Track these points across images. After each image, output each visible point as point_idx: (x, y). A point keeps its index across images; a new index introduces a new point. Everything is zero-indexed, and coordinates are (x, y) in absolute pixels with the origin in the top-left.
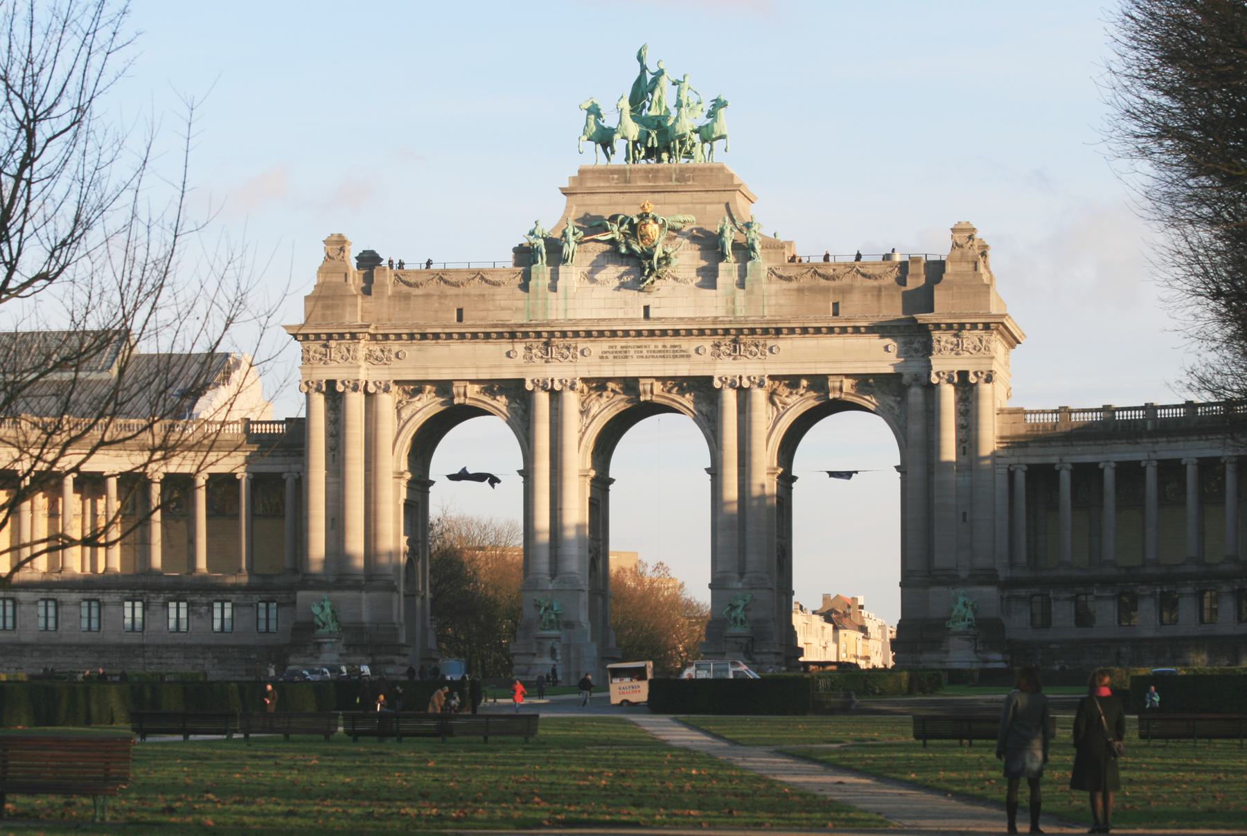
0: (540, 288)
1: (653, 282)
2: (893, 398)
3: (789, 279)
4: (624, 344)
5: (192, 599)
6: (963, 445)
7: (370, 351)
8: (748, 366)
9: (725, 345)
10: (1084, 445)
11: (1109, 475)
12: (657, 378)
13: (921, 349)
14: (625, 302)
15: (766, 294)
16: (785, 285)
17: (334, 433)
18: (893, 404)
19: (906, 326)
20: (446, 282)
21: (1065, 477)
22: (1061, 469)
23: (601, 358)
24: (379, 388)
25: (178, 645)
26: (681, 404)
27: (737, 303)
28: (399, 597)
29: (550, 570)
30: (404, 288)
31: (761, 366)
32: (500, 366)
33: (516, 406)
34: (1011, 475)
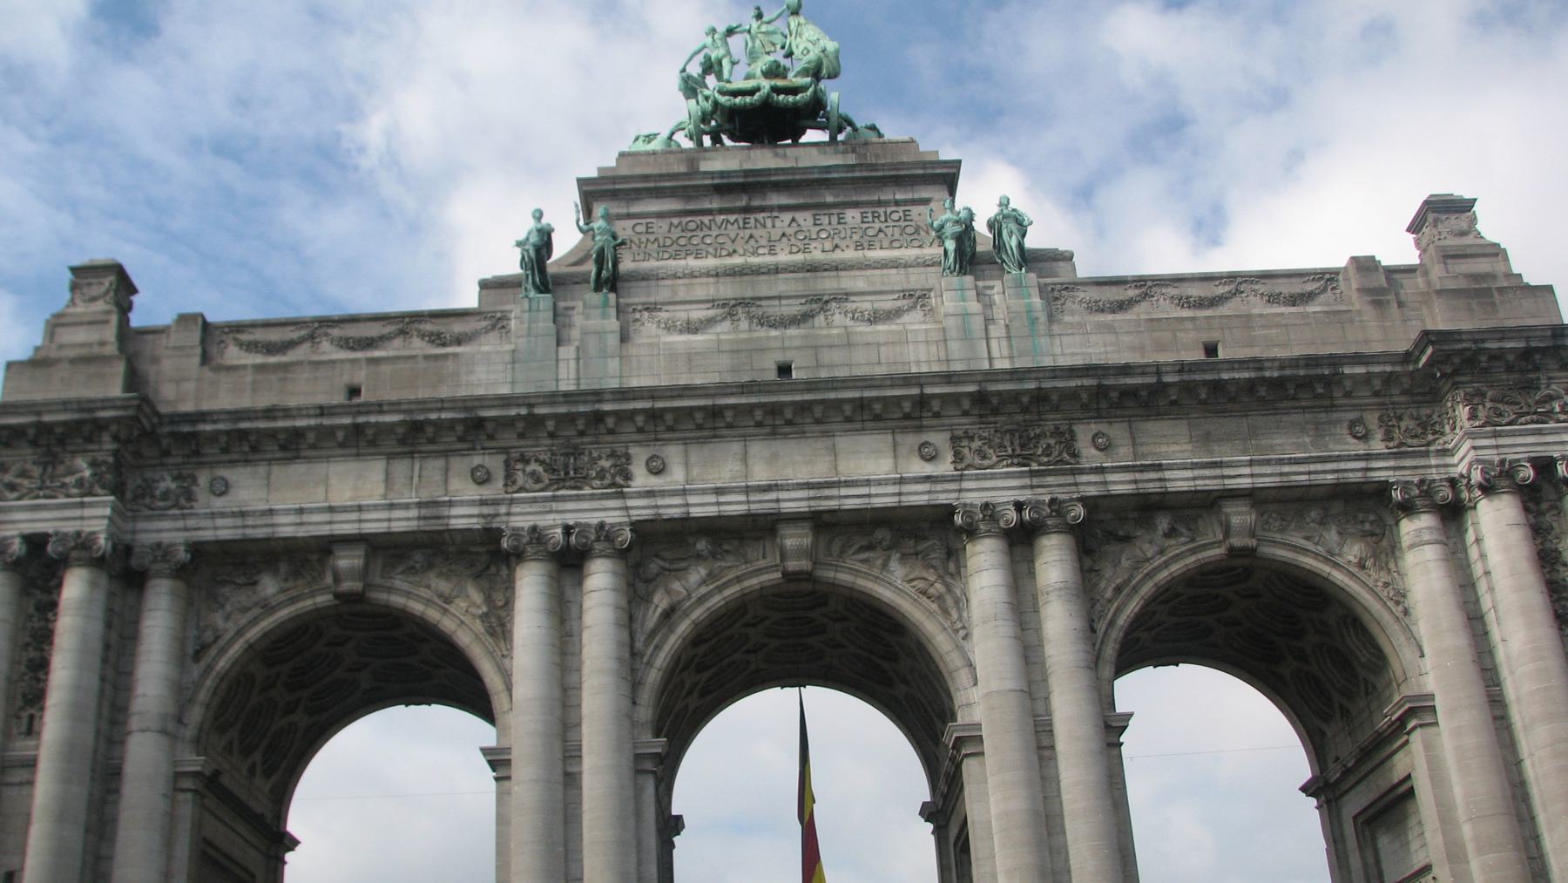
7: (145, 480)
19: (1388, 379)
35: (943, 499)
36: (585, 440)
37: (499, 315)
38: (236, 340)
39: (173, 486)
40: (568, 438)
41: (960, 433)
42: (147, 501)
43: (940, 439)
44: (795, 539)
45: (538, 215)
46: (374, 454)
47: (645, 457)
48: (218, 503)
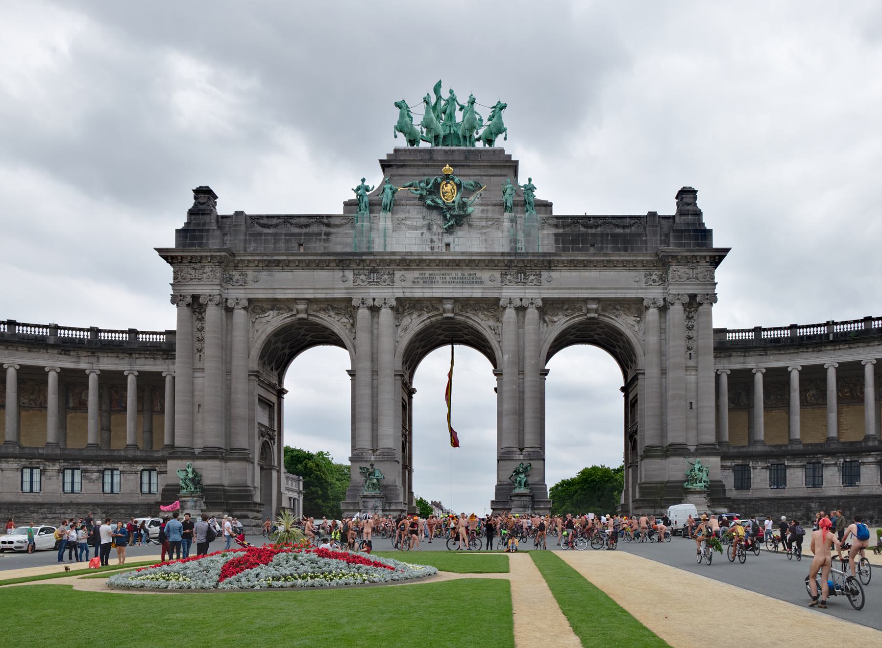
0: (364, 229)
1: (452, 225)
2: (634, 318)
3: (557, 226)
4: (431, 272)
5: (84, 467)
6: (690, 352)
8: (527, 291)
9: (510, 274)
10: (776, 354)
11: (795, 377)
12: (456, 300)
13: (657, 280)
14: (432, 241)
15: (540, 236)
16: (554, 231)
17: (200, 338)
18: (635, 323)
20: (291, 224)
21: (759, 378)
22: (757, 371)
23: (414, 282)
24: (237, 304)
25: (71, 504)
26: (474, 321)
27: (519, 245)
28: (254, 468)
29: (373, 446)
30: (259, 229)
31: (537, 291)
32: (334, 288)
33: (346, 320)
34: (718, 377)
35: (496, 296)
36: (380, 267)
37: (350, 218)
38: (257, 223)
39: (239, 278)
40: (374, 267)
41: (504, 273)
42: (231, 283)
43: (497, 274)
44: (448, 306)
45: (363, 180)
46: (309, 269)
47: (399, 275)
48: (255, 285)
